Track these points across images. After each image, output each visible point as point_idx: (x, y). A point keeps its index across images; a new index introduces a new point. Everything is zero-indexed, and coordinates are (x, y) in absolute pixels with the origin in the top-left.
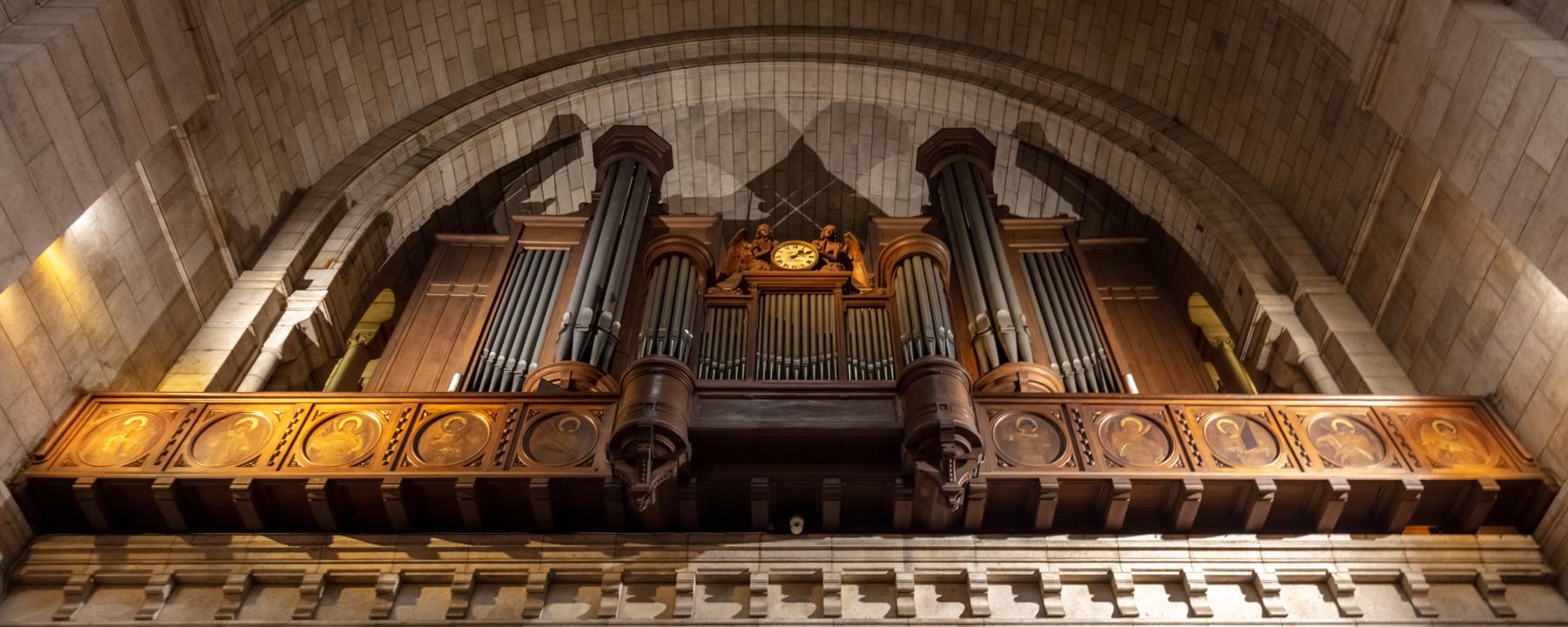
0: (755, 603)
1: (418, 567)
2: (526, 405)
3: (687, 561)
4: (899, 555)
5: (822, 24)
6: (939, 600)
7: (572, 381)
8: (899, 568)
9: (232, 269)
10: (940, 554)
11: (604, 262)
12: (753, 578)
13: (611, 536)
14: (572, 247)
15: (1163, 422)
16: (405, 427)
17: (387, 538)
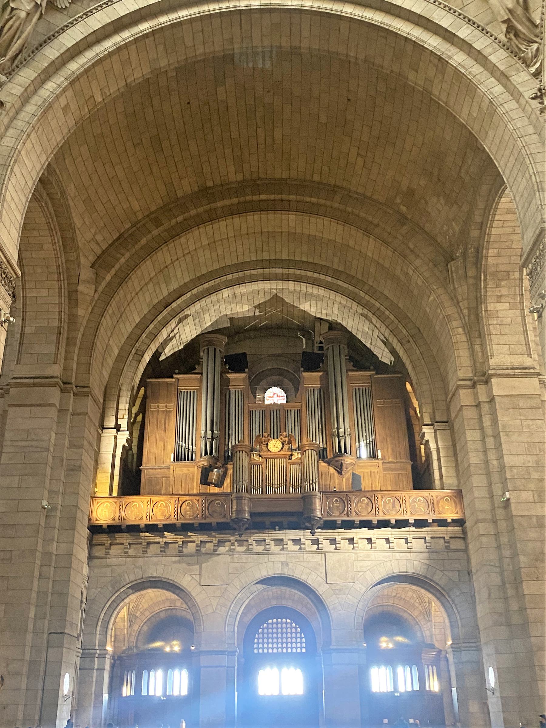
0: (267, 547)
3: (250, 537)
4: (302, 534)
5: (283, 258)
8: (302, 537)
11: (211, 404)
13: (232, 531)
14: (197, 389)
15: (371, 499)
16: (176, 506)
17: (177, 533)
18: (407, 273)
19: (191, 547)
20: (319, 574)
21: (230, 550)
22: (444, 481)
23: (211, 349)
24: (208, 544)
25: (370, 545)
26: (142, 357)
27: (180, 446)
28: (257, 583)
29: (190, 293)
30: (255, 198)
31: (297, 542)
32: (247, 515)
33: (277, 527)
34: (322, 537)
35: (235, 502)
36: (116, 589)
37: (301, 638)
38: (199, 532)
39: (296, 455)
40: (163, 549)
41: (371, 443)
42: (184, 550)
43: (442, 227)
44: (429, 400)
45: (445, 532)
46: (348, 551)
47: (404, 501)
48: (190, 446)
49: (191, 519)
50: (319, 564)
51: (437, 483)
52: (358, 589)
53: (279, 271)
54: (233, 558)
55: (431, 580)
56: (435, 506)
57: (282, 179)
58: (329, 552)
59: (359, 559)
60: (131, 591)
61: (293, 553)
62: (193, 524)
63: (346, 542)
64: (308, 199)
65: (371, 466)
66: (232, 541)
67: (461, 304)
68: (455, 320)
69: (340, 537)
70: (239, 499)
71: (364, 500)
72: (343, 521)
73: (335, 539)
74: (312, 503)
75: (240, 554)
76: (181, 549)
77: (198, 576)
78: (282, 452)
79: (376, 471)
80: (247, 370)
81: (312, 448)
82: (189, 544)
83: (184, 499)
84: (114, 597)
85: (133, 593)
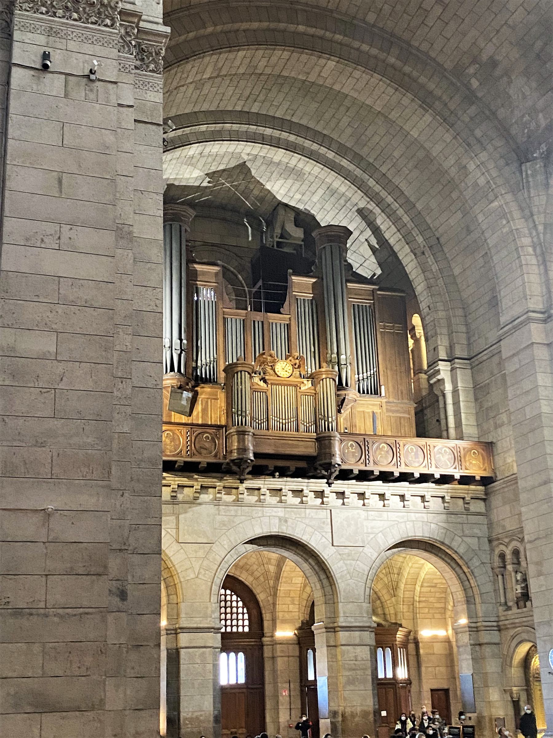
0: (262, 497)
7: (181, 385)
8: (305, 488)
10: (317, 484)
13: (219, 475)
15: (392, 447)
18: (465, 167)
21: (215, 499)
22: (464, 431)
24: (186, 490)
25: (382, 502)
30: (292, 27)
31: (298, 493)
32: (251, 456)
35: (235, 438)
37: (243, 614)
38: (177, 473)
39: (307, 385)
41: (372, 376)
43: (523, 116)
44: (445, 331)
45: (466, 492)
46: (357, 508)
47: (429, 452)
49: (173, 456)
50: (324, 523)
51: (452, 432)
52: (369, 555)
53: (268, 131)
55: (449, 547)
56: (463, 460)
57: (325, 9)
58: (334, 507)
59: (369, 518)
61: (292, 506)
63: (355, 497)
64: (356, 44)
65: (373, 405)
67: (535, 217)
68: (525, 237)
69: (350, 490)
71: (383, 447)
73: (343, 493)
74: (330, 446)
75: (227, 505)
77: (174, 531)
79: (379, 411)
81: (330, 376)
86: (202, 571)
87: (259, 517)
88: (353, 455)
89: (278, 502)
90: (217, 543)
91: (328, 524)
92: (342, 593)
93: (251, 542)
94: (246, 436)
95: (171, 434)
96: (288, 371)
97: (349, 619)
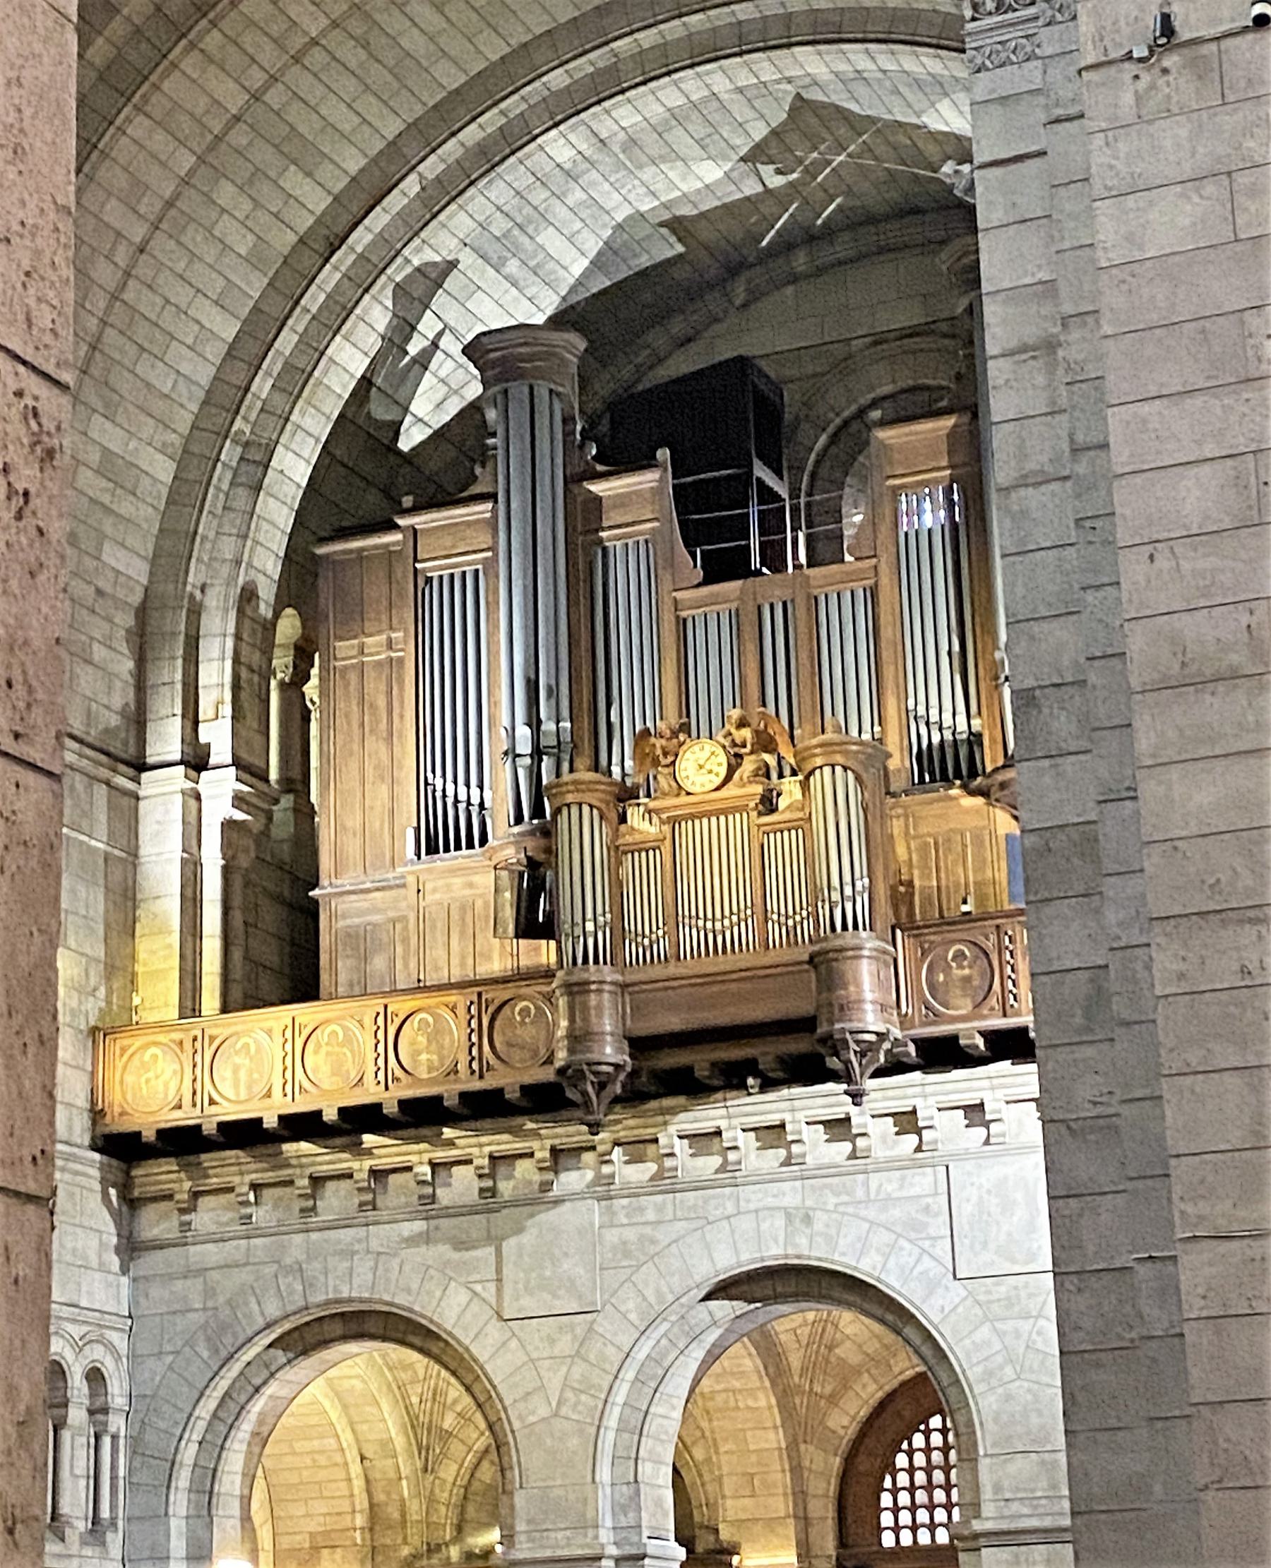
0: (732, 1156)
1: (441, 1155)
2: (480, 995)
3: (665, 1123)
6: (897, 1134)
7: (529, 858)
9: (130, 785)
10: (890, 1093)
12: (724, 1135)
19: (463, 1184)
20: (926, 1244)
21: (599, 1180)
23: (519, 391)
24: (523, 1167)
26: (267, 467)
27: (439, 794)
28: (708, 1297)
29: (413, 177)
33: (750, 1081)
34: (932, 1101)
35: (562, 1002)
36: (224, 1354)
40: (369, 1197)
42: (440, 1192)
48: (475, 792)
49: (431, 1082)
50: (927, 1209)
54: (611, 1212)
58: (964, 1156)
60: (280, 1356)
61: (828, 1171)
62: (438, 1099)
66: (600, 1148)
69: (1000, 1094)
70: (576, 990)
72: (992, 1037)
76: (429, 1190)
77: (492, 1287)
78: (731, 791)
80: (663, 454)
81: (839, 759)
82: (454, 1169)
83: (400, 1006)
84: (223, 1384)
85: (289, 1362)
86: (569, 1394)
87: (728, 1218)
88: (963, 989)
89: (782, 1165)
90: (608, 1307)
91: (937, 1215)
92: (990, 1425)
93: (723, 1290)
94: (593, 996)
95: (430, 1020)
96: (716, 769)
97: (1015, 1507)
